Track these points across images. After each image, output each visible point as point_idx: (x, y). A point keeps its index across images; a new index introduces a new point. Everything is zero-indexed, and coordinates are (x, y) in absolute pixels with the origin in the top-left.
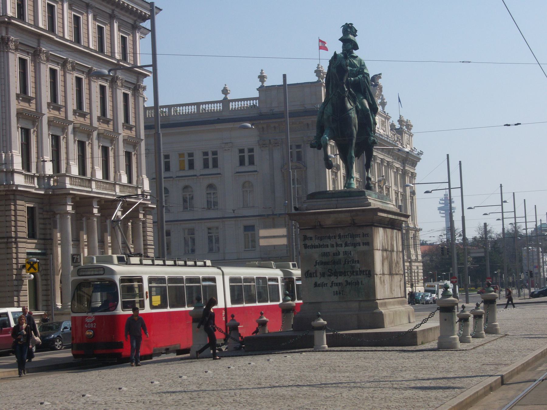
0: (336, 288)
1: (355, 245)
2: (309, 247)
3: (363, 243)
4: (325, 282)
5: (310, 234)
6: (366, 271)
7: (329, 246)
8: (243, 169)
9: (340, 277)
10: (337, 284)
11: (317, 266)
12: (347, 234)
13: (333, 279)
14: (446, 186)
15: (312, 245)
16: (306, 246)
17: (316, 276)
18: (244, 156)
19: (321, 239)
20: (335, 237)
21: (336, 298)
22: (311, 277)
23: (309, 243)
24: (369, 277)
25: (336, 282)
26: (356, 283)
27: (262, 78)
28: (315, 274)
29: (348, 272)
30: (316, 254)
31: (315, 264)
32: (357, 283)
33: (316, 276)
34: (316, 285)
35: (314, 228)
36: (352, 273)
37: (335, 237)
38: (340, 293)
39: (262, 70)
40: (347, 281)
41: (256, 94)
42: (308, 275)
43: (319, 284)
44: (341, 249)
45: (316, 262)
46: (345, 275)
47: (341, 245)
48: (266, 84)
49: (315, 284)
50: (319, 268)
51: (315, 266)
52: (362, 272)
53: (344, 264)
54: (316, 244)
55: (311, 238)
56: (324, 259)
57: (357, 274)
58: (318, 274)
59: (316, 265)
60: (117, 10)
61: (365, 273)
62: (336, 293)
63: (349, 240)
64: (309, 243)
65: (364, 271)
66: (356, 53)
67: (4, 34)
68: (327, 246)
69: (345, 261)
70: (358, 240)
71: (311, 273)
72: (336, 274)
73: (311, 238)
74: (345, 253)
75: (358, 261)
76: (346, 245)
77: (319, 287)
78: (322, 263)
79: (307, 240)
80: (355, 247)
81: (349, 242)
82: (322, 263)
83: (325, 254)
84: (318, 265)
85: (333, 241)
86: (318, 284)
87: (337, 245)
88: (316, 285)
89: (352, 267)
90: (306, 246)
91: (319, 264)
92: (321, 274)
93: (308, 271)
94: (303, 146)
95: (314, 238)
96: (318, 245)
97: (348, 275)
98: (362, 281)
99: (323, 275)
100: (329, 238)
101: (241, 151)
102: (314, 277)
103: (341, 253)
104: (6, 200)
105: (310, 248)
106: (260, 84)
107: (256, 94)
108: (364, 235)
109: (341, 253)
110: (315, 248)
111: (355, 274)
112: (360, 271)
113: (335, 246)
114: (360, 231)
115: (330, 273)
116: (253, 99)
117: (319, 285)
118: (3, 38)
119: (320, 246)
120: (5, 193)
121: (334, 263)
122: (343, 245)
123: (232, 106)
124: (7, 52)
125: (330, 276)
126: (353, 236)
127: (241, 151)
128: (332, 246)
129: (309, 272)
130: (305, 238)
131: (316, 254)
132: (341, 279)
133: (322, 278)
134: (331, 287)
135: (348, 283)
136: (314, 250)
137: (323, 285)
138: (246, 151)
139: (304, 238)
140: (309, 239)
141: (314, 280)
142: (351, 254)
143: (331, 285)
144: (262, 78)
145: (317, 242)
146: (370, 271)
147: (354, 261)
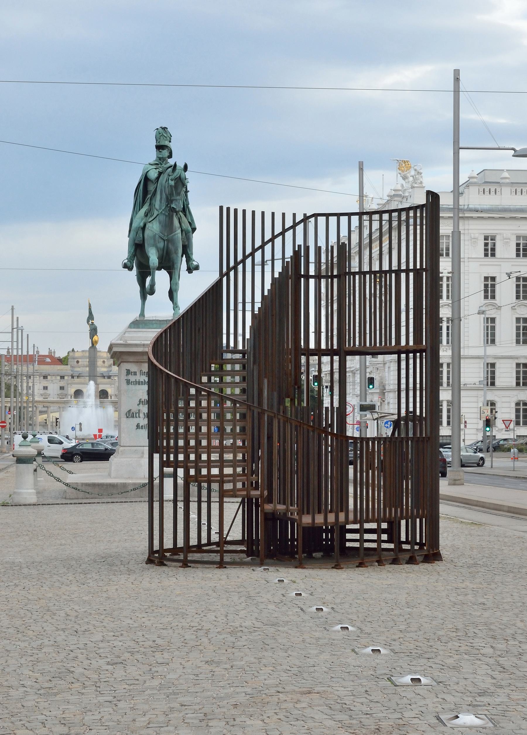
2: (132, 383)
11: (141, 405)
15: (136, 381)
16: (128, 382)
17: (139, 417)
22: (133, 417)
23: (132, 378)
28: (137, 414)
42: (129, 416)
43: (142, 426)
45: (140, 401)
49: (137, 426)
55: (135, 373)
58: (142, 415)
59: (140, 404)
73: (135, 373)
77: (142, 429)
79: (130, 375)
84: (142, 404)
86: (140, 426)
90: (128, 382)
91: (144, 403)
92: (145, 415)
93: (130, 410)
95: (138, 373)
96: (143, 381)
102: (136, 417)
105: (134, 384)
110: (139, 384)
130: (128, 372)
139: (127, 372)
140: (133, 374)
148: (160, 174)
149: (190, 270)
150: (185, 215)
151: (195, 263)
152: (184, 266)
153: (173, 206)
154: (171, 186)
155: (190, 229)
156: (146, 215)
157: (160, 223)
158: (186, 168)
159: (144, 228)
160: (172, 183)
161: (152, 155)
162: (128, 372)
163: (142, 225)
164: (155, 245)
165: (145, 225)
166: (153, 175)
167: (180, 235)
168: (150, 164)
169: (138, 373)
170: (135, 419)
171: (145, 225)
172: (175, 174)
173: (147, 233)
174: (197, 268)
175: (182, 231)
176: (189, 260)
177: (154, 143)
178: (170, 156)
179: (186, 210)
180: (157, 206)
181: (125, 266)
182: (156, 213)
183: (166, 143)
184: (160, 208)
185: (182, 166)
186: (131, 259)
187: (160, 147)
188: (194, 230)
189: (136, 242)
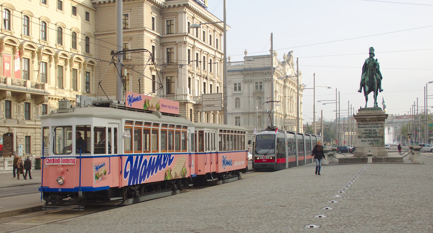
0: (370, 142)
1: (377, 127)
3: (381, 127)
5: (360, 123)
8: (236, 92)
9: (371, 138)
13: (369, 139)
16: (359, 127)
18: (236, 87)
19: (365, 125)
21: (370, 145)
23: (360, 126)
27: (246, 53)
30: (363, 130)
34: (362, 141)
35: (362, 121)
36: (376, 137)
37: (370, 124)
41: (243, 60)
44: (372, 129)
48: (247, 55)
50: (364, 135)
52: (380, 137)
53: (373, 134)
55: (361, 125)
56: (366, 132)
57: (378, 138)
58: (363, 137)
68: (367, 127)
70: (378, 125)
72: (370, 137)
74: (374, 130)
76: (374, 127)
78: (365, 133)
80: (377, 128)
81: (375, 126)
82: (365, 133)
83: (366, 130)
85: (370, 126)
87: (371, 127)
88: (362, 141)
89: (376, 135)
90: (359, 127)
93: (359, 136)
94: (263, 83)
95: (362, 124)
99: (365, 137)
100: (368, 124)
101: (235, 84)
103: (372, 130)
106: (245, 55)
107: (243, 60)
108: (382, 124)
109: (372, 130)
112: (379, 136)
114: (380, 122)
116: (241, 62)
119: (364, 127)
121: (369, 133)
123: (232, 64)
125: (367, 138)
126: (377, 124)
127: (235, 84)
128: (369, 127)
130: (359, 124)
131: (363, 130)
132: (372, 139)
133: (365, 139)
134: (368, 141)
136: (362, 129)
137: (365, 141)
138: (237, 84)
141: (361, 139)
144: (246, 53)
145: (363, 126)
146: (383, 136)
147: (377, 133)
148: (369, 62)
149: (380, 91)
150: (379, 74)
151: (382, 89)
152: (379, 90)
153: (373, 72)
154: (372, 66)
155: (380, 78)
156: (365, 75)
158: (377, 60)
159: (364, 79)
160: (372, 65)
161: (368, 56)
163: (364, 78)
164: (368, 85)
165: (365, 78)
166: (367, 63)
167: (376, 81)
168: (367, 59)
169: (362, 124)
170: (361, 139)
171: (365, 78)
172: (374, 62)
173: (366, 81)
174: (382, 90)
175: (377, 79)
176: (380, 88)
177: (369, 52)
178: (374, 56)
179: (379, 72)
180: (368, 72)
181: (359, 91)
182: (368, 74)
183: (373, 52)
184: (369, 73)
185: (376, 59)
186: (361, 89)
187: (370, 54)
188: (382, 78)
189: (362, 84)
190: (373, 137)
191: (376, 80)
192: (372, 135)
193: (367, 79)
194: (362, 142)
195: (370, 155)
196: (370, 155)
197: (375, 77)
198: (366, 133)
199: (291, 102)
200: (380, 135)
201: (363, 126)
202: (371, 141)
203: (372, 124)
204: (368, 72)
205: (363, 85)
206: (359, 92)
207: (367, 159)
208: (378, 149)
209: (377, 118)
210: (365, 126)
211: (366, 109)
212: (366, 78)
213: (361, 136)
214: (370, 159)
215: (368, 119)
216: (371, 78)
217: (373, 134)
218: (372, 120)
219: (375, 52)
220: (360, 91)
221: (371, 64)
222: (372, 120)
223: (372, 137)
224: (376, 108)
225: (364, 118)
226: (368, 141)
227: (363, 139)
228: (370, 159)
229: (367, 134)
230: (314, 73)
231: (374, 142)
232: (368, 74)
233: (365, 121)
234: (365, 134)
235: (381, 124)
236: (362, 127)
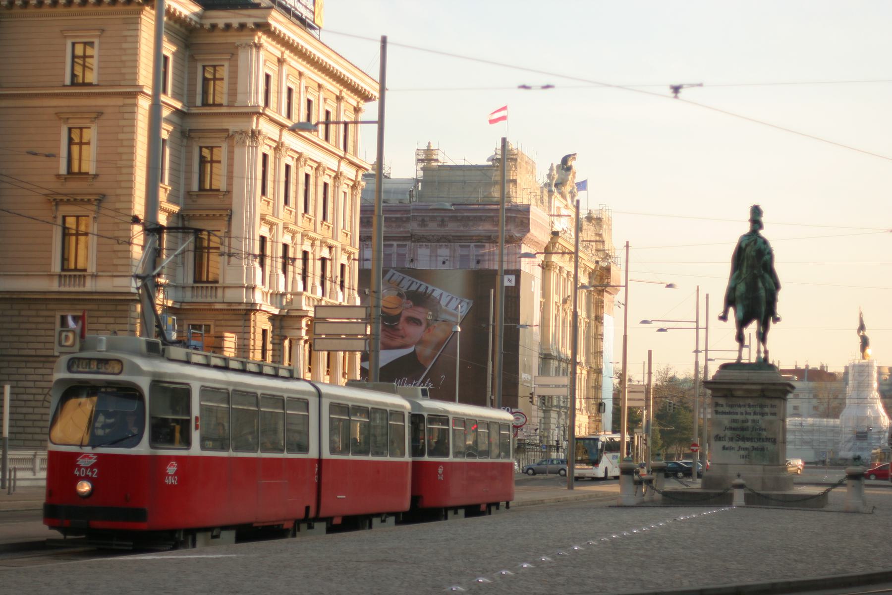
0: (742, 453)
1: (763, 414)
4: (734, 446)
5: (721, 401)
6: (772, 438)
7: (739, 413)
10: (744, 448)
11: (726, 431)
12: (756, 404)
13: (741, 444)
14: (694, 325)
16: (717, 412)
19: (731, 406)
20: (745, 406)
21: (742, 461)
23: (720, 409)
24: (774, 444)
25: (743, 447)
26: (761, 449)
29: (755, 438)
30: (726, 420)
31: (724, 429)
32: (762, 449)
33: (725, 440)
35: (725, 396)
36: (760, 439)
38: (746, 457)
39: (429, 143)
40: (753, 447)
44: (750, 417)
45: (726, 428)
46: (752, 441)
47: (750, 414)
50: (729, 433)
51: (725, 430)
52: (768, 440)
53: (752, 431)
54: (727, 411)
55: (722, 406)
56: (735, 425)
57: (763, 441)
58: (727, 438)
60: (345, 90)
61: (770, 441)
62: (743, 457)
63: (758, 409)
64: (720, 409)
65: (769, 439)
66: (762, 233)
67: (254, 128)
69: (753, 429)
70: (767, 410)
71: (720, 438)
72: (744, 439)
74: (754, 421)
75: (765, 429)
76: (755, 413)
83: (734, 421)
85: (742, 410)
87: (747, 413)
88: (724, 448)
89: (760, 434)
90: (717, 412)
97: (755, 441)
98: (767, 448)
99: (731, 439)
100: (740, 406)
104: (245, 320)
111: (761, 440)
113: (744, 414)
115: (737, 439)
117: (727, 449)
118: (253, 132)
119: (729, 413)
120: (245, 312)
121: (743, 429)
122: (752, 414)
124: (256, 147)
125: (738, 441)
126: (762, 406)
128: (742, 414)
129: (719, 436)
130: (717, 405)
131: (726, 420)
132: (748, 444)
135: (754, 449)
136: (724, 416)
142: (758, 423)
143: (738, 449)
145: (727, 409)
147: (761, 429)
153: (755, 272)
157: (746, 284)
160: (753, 254)
162: (717, 405)
163: (733, 285)
166: (744, 245)
173: (738, 293)
180: (744, 271)
182: (743, 276)
183: (758, 218)
184: (746, 273)
186: (726, 312)
190: (750, 439)
191: (762, 293)
192: (747, 434)
193: (741, 288)
194: (725, 451)
195: (741, 486)
196: (741, 486)
197: (760, 285)
198: (734, 429)
199: (566, 313)
200: (770, 436)
201: (727, 409)
202: (746, 449)
203: (749, 406)
204: (744, 271)
205: (730, 301)
206: (722, 322)
207: (731, 495)
208: (764, 470)
209: (763, 391)
210: (732, 410)
211: (738, 365)
212: (739, 286)
213: (722, 435)
214: (739, 497)
215: (739, 393)
216: (752, 287)
217: (752, 431)
218: (749, 394)
219: (764, 219)
220: (724, 318)
221: (750, 252)
222: (749, 394)
223: (748, 439)
224: (763, 364)
225: (730, 390)
226: (738, 450)
227: (727, 444)
228: (739, 497)
229: (734, 432)
230: (627, 242)
231: (754, 453)
232: (743, 276)
233: (733, 396)
234: (731, 432)
235: (772, 406)
236: (724, 413)
